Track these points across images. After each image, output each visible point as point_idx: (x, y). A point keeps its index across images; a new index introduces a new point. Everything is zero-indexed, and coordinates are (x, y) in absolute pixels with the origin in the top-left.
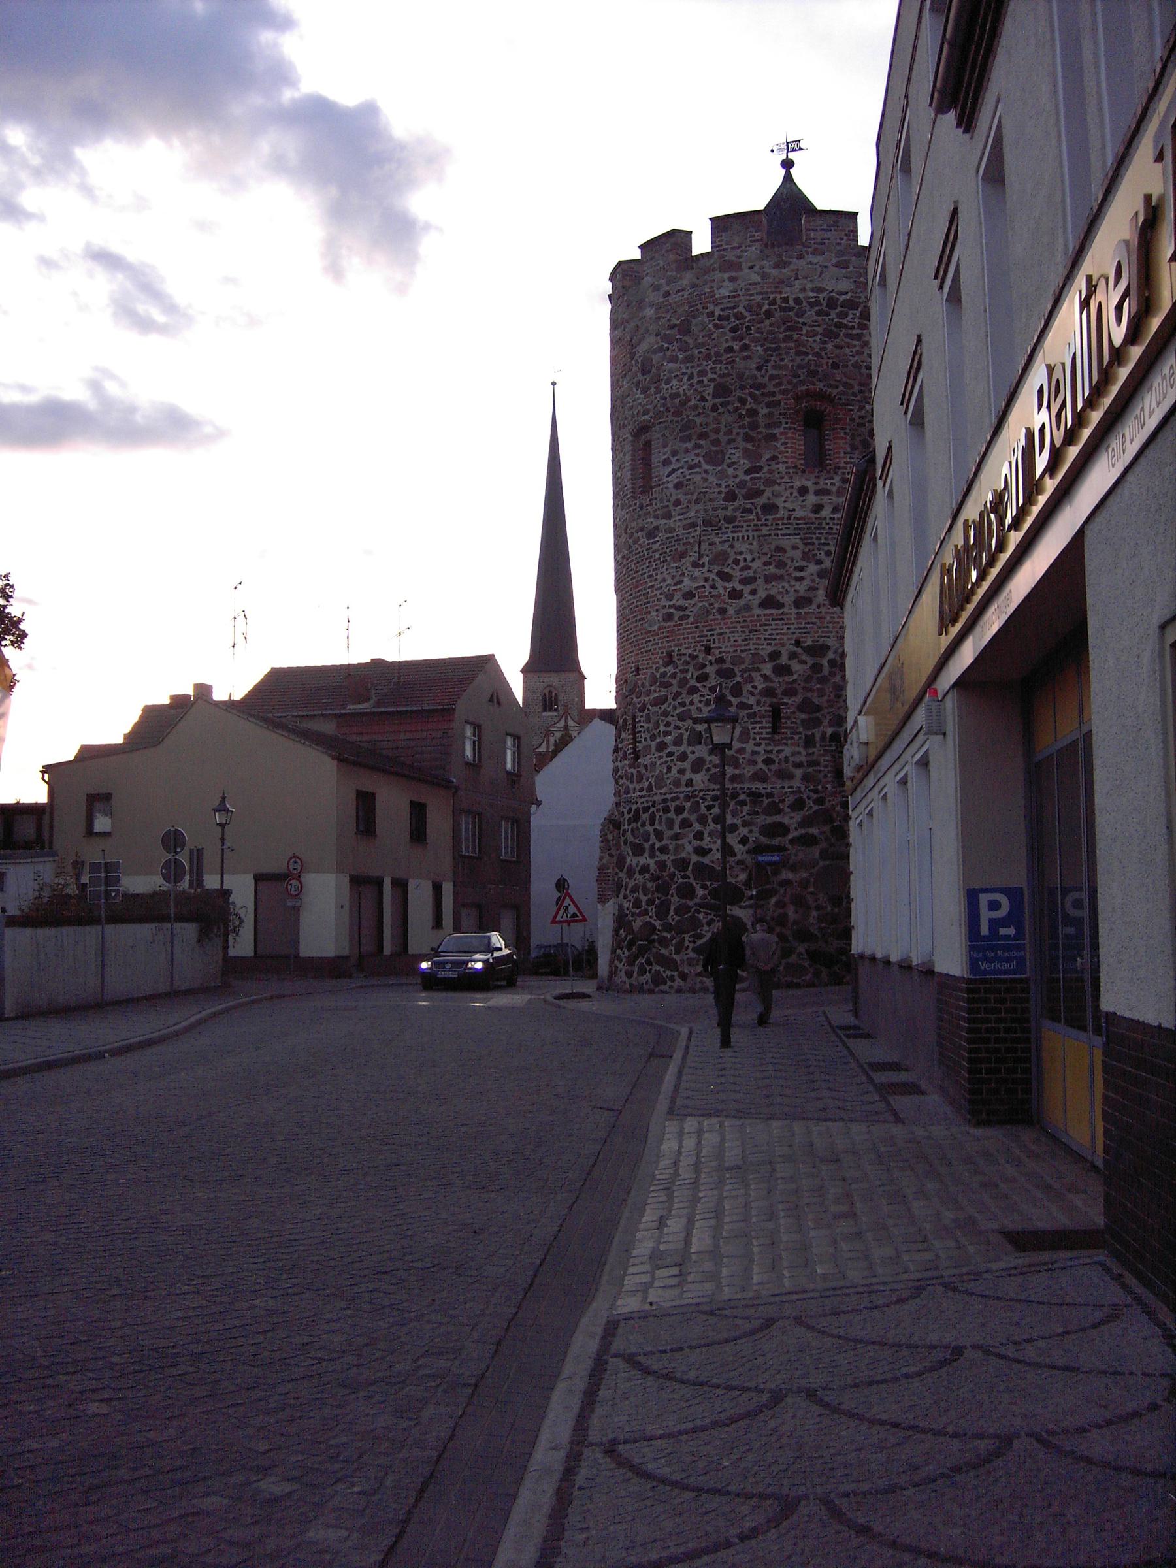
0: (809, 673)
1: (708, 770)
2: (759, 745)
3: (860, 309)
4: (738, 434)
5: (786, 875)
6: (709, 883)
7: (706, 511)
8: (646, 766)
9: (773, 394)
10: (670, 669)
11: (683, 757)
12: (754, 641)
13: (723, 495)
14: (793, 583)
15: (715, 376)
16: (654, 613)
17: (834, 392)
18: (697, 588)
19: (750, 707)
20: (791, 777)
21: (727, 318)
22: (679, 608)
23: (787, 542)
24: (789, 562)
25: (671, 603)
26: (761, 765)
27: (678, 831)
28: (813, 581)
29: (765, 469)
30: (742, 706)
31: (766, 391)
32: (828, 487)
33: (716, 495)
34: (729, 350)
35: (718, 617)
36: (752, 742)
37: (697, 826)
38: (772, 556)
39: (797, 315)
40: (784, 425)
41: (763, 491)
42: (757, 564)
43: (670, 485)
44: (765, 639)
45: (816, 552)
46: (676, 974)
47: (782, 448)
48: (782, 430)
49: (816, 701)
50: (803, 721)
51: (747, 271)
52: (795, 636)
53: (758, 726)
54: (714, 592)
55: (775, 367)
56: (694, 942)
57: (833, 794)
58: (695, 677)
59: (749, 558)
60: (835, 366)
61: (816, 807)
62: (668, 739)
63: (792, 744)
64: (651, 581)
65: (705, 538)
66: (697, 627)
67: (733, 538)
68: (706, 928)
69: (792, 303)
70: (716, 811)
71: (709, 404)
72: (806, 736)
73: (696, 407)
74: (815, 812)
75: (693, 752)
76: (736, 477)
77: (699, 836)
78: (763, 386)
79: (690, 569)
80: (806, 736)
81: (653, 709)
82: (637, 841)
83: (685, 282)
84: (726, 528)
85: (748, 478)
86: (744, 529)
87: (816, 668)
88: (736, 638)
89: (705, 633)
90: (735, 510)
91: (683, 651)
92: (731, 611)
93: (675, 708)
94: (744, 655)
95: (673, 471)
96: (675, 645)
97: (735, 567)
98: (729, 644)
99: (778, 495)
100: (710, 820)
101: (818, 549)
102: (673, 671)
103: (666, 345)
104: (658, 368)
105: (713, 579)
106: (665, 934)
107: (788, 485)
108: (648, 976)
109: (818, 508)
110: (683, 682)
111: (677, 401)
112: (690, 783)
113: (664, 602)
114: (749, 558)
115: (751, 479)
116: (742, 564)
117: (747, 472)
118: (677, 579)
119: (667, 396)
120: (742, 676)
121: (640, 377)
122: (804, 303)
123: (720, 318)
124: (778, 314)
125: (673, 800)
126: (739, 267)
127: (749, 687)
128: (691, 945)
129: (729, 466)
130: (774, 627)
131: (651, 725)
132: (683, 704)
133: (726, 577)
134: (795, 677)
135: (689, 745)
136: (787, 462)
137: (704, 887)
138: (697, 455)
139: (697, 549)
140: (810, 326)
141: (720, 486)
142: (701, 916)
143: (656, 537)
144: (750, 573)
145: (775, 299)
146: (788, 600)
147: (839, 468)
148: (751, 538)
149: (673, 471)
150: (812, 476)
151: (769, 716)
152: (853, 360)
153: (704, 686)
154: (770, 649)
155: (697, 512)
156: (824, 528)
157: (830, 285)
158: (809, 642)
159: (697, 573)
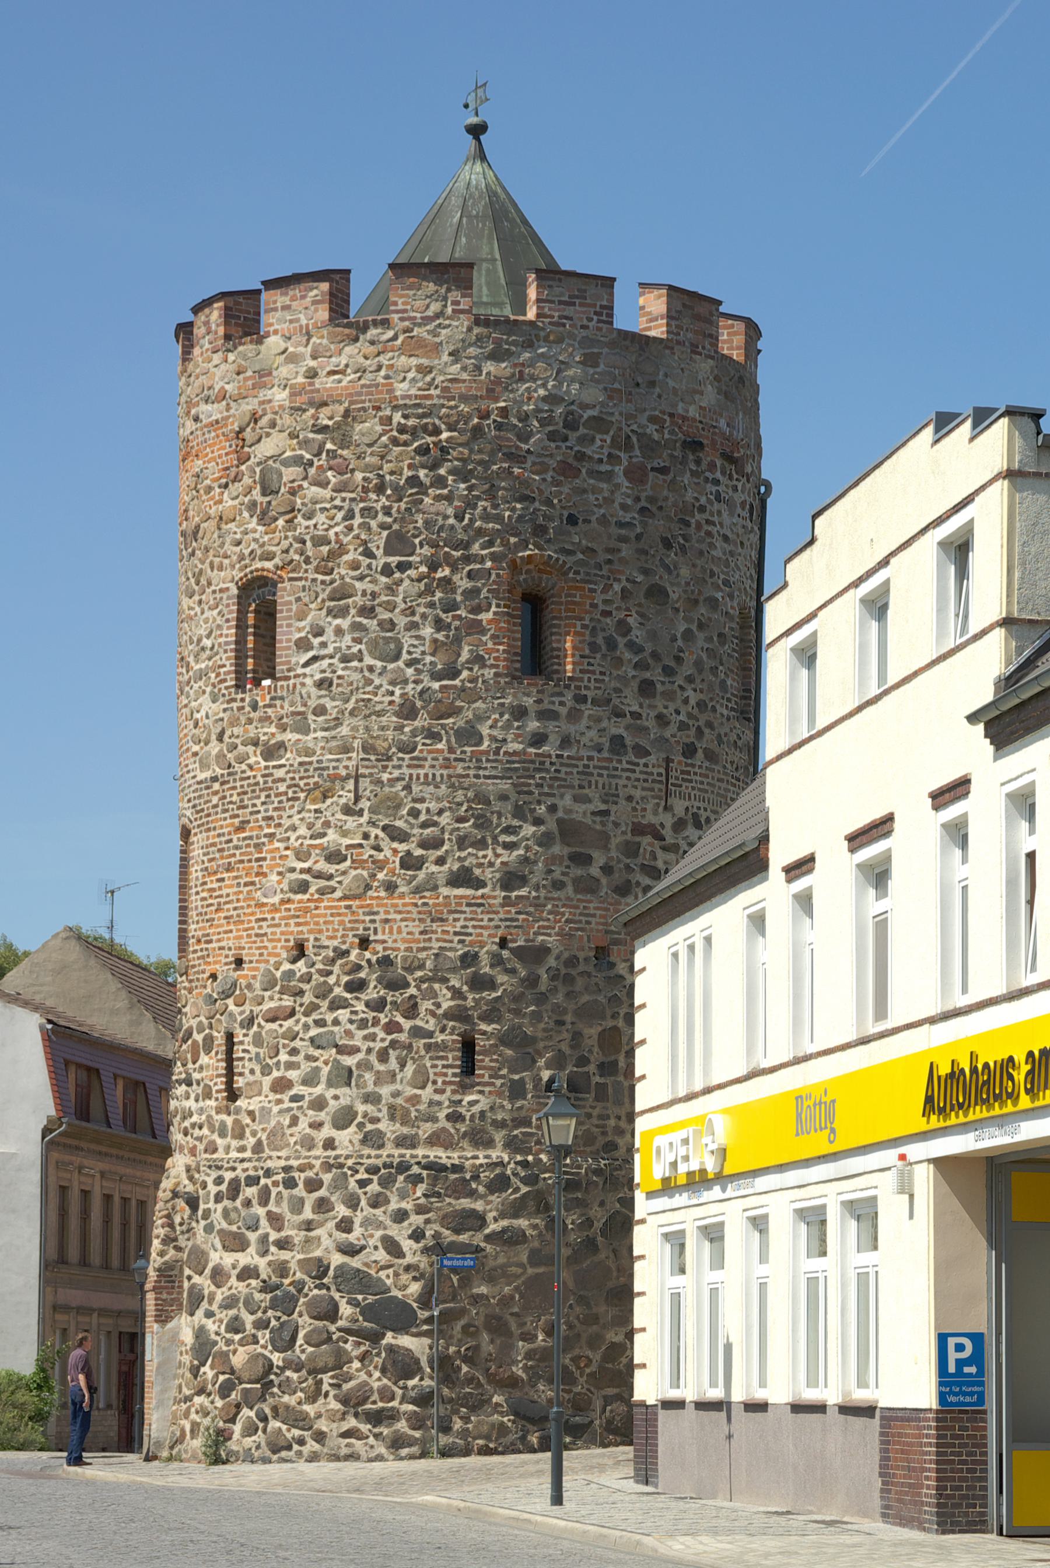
2: (442, 1092)
7: (367, 729)
10: (301, 966)
11: (319, 1104)
12: (439, 935)
22: (319, 876)
25: (306, 865)
26: (443, 1123)
30: (417, 1032)
35: (383, 894)
36: (430, 1088)
37: (342, 1210)
42: (445, 819)
43: (308, 681)
53: (440, 1063)
62: (293, 1075)
65: (367, 771)
67: (411, 775)
73: (355, 566)
85: (436, 685)
86: (427, 764)
88: (410, 929)
89: (362, 917)
93: (306, 1027)
94: (422, 955)
96: (310, 932)
102: (304, 970)
103: (308, 456)
105: (376, 837)
111: (325, 549)
112: (329, 1144)
116: (423, 817)
125: (301, 1169)
129: (409, 664)
135: (330, 1084)
139: (350, 785)
148: (438, 779)
149: (315, 659)
155: (354, 729)
159: (351, 822)
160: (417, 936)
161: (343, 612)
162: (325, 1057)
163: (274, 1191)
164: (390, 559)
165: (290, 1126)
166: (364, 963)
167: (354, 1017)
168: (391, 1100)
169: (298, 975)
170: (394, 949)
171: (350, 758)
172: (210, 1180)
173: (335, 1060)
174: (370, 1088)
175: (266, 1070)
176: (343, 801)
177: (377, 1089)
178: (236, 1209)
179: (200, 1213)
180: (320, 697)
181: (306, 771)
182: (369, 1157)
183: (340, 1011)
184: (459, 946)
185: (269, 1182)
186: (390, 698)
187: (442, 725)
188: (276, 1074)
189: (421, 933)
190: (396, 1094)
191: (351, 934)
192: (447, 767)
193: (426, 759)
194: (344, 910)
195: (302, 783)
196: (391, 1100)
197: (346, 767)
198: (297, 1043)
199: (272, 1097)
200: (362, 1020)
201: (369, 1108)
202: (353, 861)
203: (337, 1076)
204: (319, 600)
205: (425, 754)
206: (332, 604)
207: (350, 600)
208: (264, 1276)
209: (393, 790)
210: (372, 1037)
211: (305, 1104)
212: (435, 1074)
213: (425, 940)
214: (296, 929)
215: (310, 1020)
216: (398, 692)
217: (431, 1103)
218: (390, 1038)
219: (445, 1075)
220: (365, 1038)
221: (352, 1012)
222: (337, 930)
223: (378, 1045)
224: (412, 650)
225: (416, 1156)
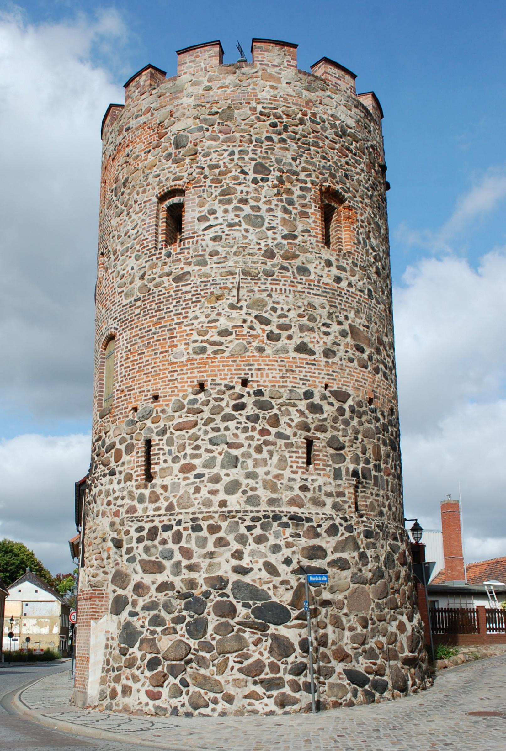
1: (244, 492)
2: (296, 472)
4: (277, 205)
6: (251, 602)
10: (202, 397)
11: (216, 479)
12: (291, 379)
13: (262, 252)
14: (322, 336)
18: (233, 327)
19: (288, 438)
22: (214, 343)
23: (317, 300)
24: (318, 317)
26: (297, 492)
29: (300, 238)
30: (279, 435)
33: (256, 251)
34: (269, 139)
35: (256, 354)
36: (288, 470)
37: (235, 546)
38: (305, 310)
39: (322, 128)
41: (298, 256)
42: (292, 314)
43: (207, 238)
44: (300, 379)
49: (341, 439)
50: (332, 456)
53: (294, 455)
54: (253, 332)
55: (306, 162)
63: (324, 475)
65: (245, 285)
68: (252, 647)
70: (258, 531)
72: (335, 469)
73: (236, 178)
74: (346, 538)
75: (227, 475)
77: (238, 555)
79: (227, 309)
84: (265, 279)
85: (285, 242)
86: (281, 283)
87: (341, 411)
88: (274, 375)
89: (243, 367)
91: (218, 381)
92: (269, 351)
93: (206, 432)
94: (282, 390)
95: (211, 226)
96: (208, 376)
97: (272, 313)
98: (267, 379)
99: (309, 262)
100: (251, 540)
102: (204, 398)
107: (318, 255)
108: (185, 699)
111: (217, 171)
112: (223, 504)
113: (195, 337)
114: (286, 308)
115: (289, 243)
116: (279, 312)
117: (284, 237)
118: (213, 317)
120: (279, 409)
122: (326, 123)
123: (262, 114)
130: (307, 370)
132: (218, 430)
133: (265, 321)
134: (325, 416)
135: (223, 466)
137: (246, 605)
139: (235, 292)
146: (318, 349)
148: (288, 291)
149: (211, 226)
153: (241, 415)
154: (305, 388)
158: (335, 388)
159: (234, 313)
160: (278, 379)
161: (229, 202)
162: (220, 450)
163: (185, 534)
164: (257, 176)
165: (194, 493)
166: (245, 394)
167: (239, 426)
168: (265, 477)
169: (200, 401)
170: (264, 386)
171: (234, 278)
173: (227, 452)
174: (251, 469)
176: (230, 301)
177: (255, 470)
178: (155, 546)
179: (124, 550)
180: (214, 246)
181: (205, 286)
182: (252, 512)
183: (230, 423)
184: (303, 386)
185: (181, 528)
186: (259, 247)
187: (289, 263)
189: (280, 377)
190: (267, 473)
191: (236, 377)
192: (293, 286)
193: (280, 281)
194: (231, 363)
195: (202, 293)
196: (265, 477)
197: (232, 283)
198: (199, 442)
200: (245, 427)
201: (250, 481)
202: (237, 335)
203: (228, 462)
204: (213, 196)
205: (280, 278)
206: (222, 198)
207: (233, 196)
209: (261, 296)
210: (252, 438)
211: (205, 479)
212: (292, 462)
213: (283, 382)
214: (198, 375)
215: (208, 428)
216: (263, 244)
217: (290, 480)
218: (263, 438)
219: (298, 462)
220: (247, 438)
221: (238, 423)
222: (227, 375)
223: (254, 443)
224: (271, 222)
225: (282, 512)
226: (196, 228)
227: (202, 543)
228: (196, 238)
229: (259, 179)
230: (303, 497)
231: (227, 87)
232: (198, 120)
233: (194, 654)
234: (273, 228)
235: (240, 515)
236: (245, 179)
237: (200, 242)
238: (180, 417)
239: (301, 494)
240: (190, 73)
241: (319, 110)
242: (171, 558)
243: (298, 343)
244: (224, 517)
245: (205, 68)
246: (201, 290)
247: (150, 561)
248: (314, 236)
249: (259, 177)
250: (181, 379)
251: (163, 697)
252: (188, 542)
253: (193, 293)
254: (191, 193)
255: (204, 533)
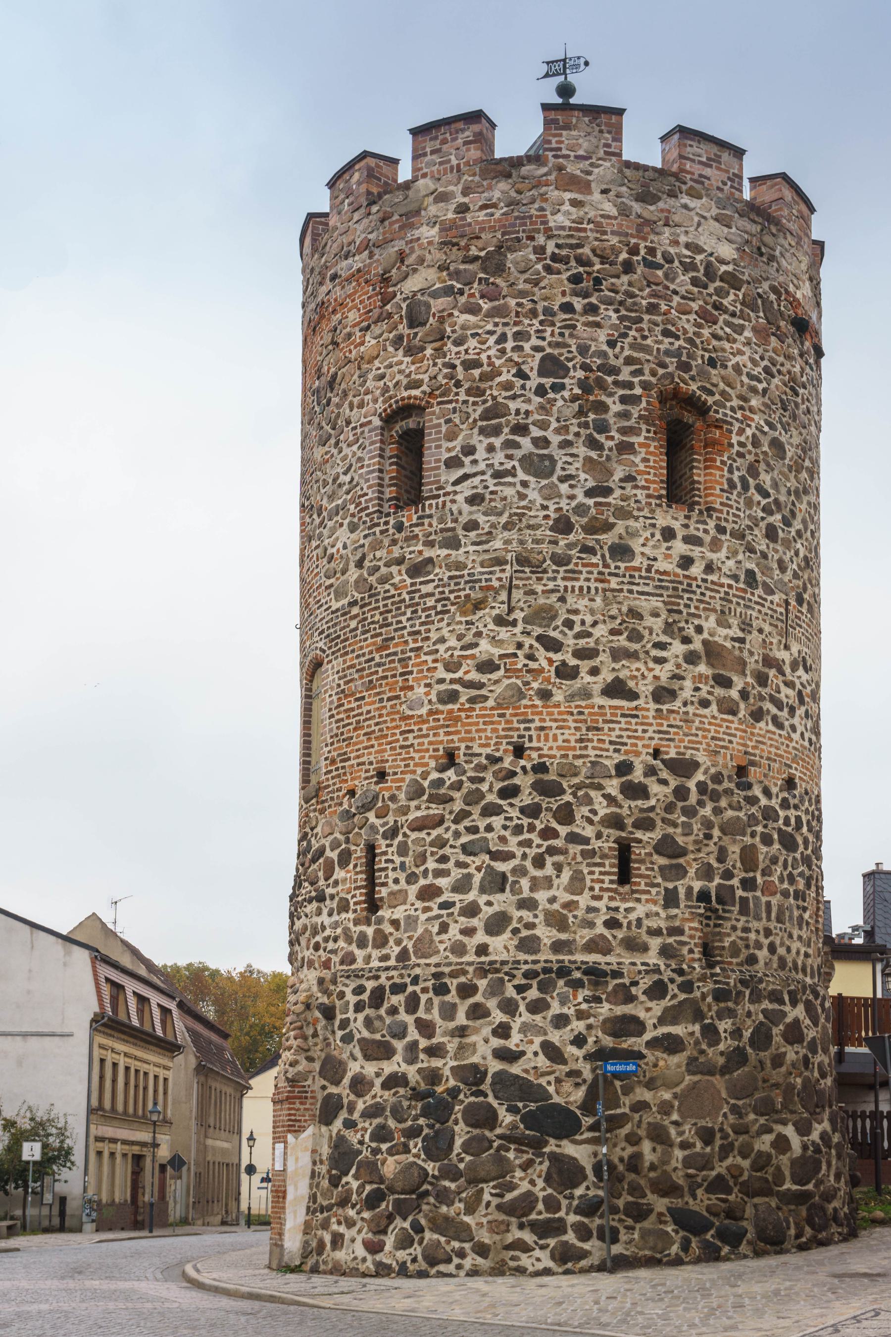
0: (671, 798)
1: (516, 931)
2: (599, 898)
3: (743, 290)
4: (577, 434)
5: (642, 1094)
6: (520, 1105)
7: (521, 542)
8: (395, 923)
9: (630, 385)
10: (450, 775)
11: (471, 910)
12: (595, 744)
13: (551, 523)
14: (651, 665)
15: (544, 344)
16: (421, 690)
17: (710, 400)
18: (501, 657)
19: (586, 841)
20: (645, 948)
21: (565, 260)
22: (470, 685)
23: (644, 604)
24: (646, 633)
25: (456, 676)
26: (600, 929)
27: (465, 1022)
28: (678, 666)
29: (618, 493)
30: (573, 838)
31: (620, 378)
32: (700, 534)
33: (539, 521)
34: (567, 308)
35: (538, 702)
36: (587, 894)
37: (498, 1016)
38: (624, 621)
39: (666, 276)
40: (644, 434)
41: (613, 525)
42: (600, 631)
43: (460, 498)
44: (611, 743)
45: (682, 624)
46: (467, 1246)
47: (642, 467)
48: (641, 439)
49: (680, 840)
50: (661, 868)
51: (597, 196)
52: (653, 743)
53: (597, 870)
54: (533, 665)
55: (632, 346)
56: (501, 1196)
57: (703, 978)
58: (495, 789)
59: (589, 619)
60: (712, 363)
61: (682, 996)
62: (442, 882)
63: (647, 901)
64: (415, 641)
65: (520, 583)
66: (500, 715)
67: (566, 587)
68: (519, 1174)
69: (659, 259)
70: (533, 994)
71: (532, 384)
72: (666, 889)
73: (508, 386)
74: (680, 1003)
75: (489, 904)
76: (572, 497)
77: (503, 1031)
78: (614, 371)
79: (491, 626)
80: (666, 889)
81: (414, 835)
82: (378, 1037)
83: (497, 194)
84: (554, 571)
85: (591, 502)
86: (582, 577)
87: (681, 793)
88: (566, 737)
89: (516, 725)
90: (570, 546)
91: (477, 750)
92: (558, 696)
93: (457, 835)
94: (579, 762)
95: (466, 477)
96: (461, 740)
97: (566, 630)
98: (555, 745)
99: (633, 534)
100: (522, 1008)
101: (687, 622)
102: (454, 778)
103: (459, 286)
104: (441, 320)
105: (531, 647)
106: (447, 1183)
107: (649, 521)
108: (417, 1250)
109: (686, 562)
110: (474, 798)
111: (476, 373)
112: (482, 950)
113: (441, 673)
114: (589, 619)
115: (597, 504)
116: (577, 628)
117: (589, 493)
118: (469, 638)
119: (457, 362)
120: (574, 794)
121: (403, 329)
122: (676, 263)
123: (555, 258)
124: (640, 269)
125: (453, 975)
126: (586, 187)
127: (585, 810)
128: (495, 1201)
129: (562, 480)
130: (623, 726)
131: (409, 860)
132: (473, 830)
133: (553, 645)
134: (653, 802)
135: (483, 890)
136: (648, 488)
137: (512, 1110)
138: (510, 457)
139: (504, 596)
140: (683, 297)
141: (545, 508)
142: (511, 1155)
143: (429, 573)
144: (590, 642)
145: (637, 246)
146: (645, 688)
147: (714, 510)
148: (593, 591)
149: (466, 477)
150: (681, 515)
151: (615, 857)
152: (734, 360)
153: (511, 805)
154: (618, 758)
155: (507, 542)
156: (694, 592)
157: (707, 241)
158: (672, 754)
159: (503, 633)
160: (573, 744)
161: (496, 431)
162: (478, 863)
163: (424, 998)
164: (543, 380)
165: (439, 934)
166: (518, 770)
167: (508, 823)
168: (548, 906)
169: (448, 783)
170: (550, 757)
171: (503, 571)
172: (348, 991)
173: (489, 866)
174: (526, 893)
175: (412, 878)
176: (497, 611)
177: (532, 895)
178: (380, 1018)
180: (471, 513)
181: (456, 584)
182: (526, 962)
183: (494, 818)
184: (616, 755)
185: (417, 989)
186: (545, 513)
187: (597, 541)
188: (422, 882)
189: (577, 741)
190: (553, 900)
191: (504, 741)
192: (602, 581)
193: (581, 572)
194: (496, 719)
195: (452, 596)
196: (548, 906)
197: (500, 579)
198: (447, 851)
199: (419, 904)
200: (517, 826)
201: (525, 913)
202: (507, 670)
203: (490, 882)
204: (471, 420)
205: (580, 568)
206: (485, 423)
207: (503, 420)
208: (412, 1083)
209: (548, 602)
210: (528, 843)
211: (456, 910)
212: (593, 881)
213: (581, 748)
214: (445, 738)
215: (461, 827)
216: (552, 508)
217: (590, 910)
218: (546, 844)
219: (602, 881)
220: (520, 844)
221: (506, 819)
222: (491, 738)
223: (532, 852)
224: (566, 466)
225: (575, 962)
226: (443, 479)
227: (449, 1012)
228: (442, 499)
229: (548, 386)
230: (610, 938)
231: (494, 206)
232: (445, 273)
233: (431, 1184)
234: (570, 477)
235: (506, 968)
236: (523, 387)
237: (448, 504)
238: (418, 808)
239: (607, 933)
240: (432, 177)
241: (663, 239)
242: (404, 1037)
243: (609, 680)
244: (482, 972)
245: (458, 165)
246: (451, 592)
247: (374, 1041)
248: (644, 488)
249: (548, 382)
250: (419, 744)
251: (388, 1247)
252: (428, 1010)
253: (437, 596)
254: (434, 413)
255: (452, 997)
